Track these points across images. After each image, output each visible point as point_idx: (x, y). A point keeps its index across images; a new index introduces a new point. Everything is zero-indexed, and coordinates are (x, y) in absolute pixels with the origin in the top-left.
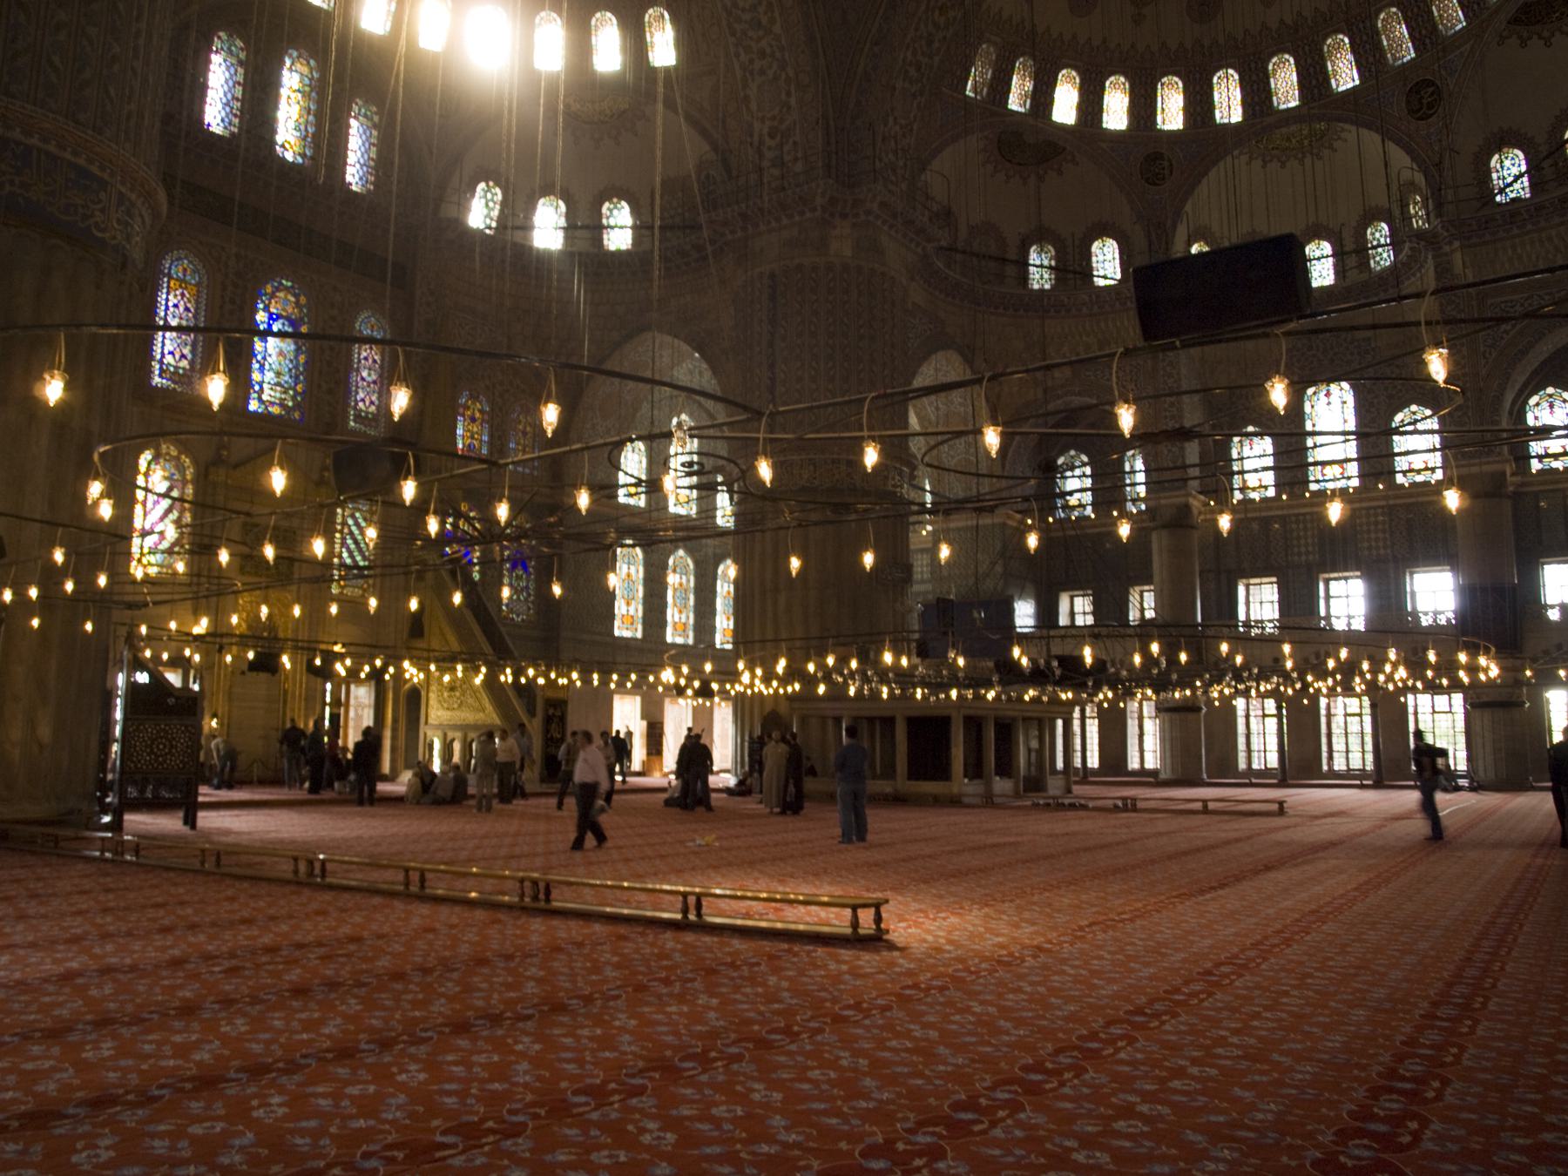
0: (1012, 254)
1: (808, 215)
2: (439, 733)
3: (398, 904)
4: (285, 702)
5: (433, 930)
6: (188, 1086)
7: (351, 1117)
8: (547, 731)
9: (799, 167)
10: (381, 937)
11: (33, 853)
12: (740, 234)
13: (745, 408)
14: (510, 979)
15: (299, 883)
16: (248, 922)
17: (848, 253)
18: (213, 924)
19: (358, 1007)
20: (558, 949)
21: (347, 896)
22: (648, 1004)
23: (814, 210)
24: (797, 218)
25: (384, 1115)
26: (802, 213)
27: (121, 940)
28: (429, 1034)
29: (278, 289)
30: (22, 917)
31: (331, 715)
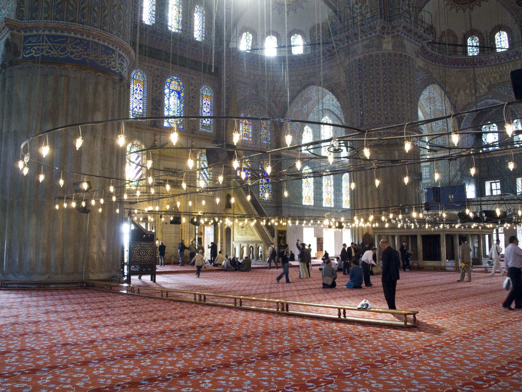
0: (460, 42)
1: (373, 34)
2: (238, 244)
3: (233, 312)
4: (182, 234)
5: (247, 321)
6: (178, 375)
7: (233, 388)
8: (279, 242)
9: (369, 15)
10: (230, 324)
11: (104, 292)
12: (346, 44)
13: (359, 130)
14: (278, 340)
15: (196, 303)
16: (182, 317)
17: (391, 48)
18: (171, 319)
19: (227, 350)
20: (294, 329)
21: (214, 308)
22: (330, 350)
23: (376, 32)
24: (369, 36)
25: (244, 387)
26: (371, 34)
27: (142, 324)
28: (254, 360)
29: (172, 80)
30: (107, 315)
31: (199, 238)
